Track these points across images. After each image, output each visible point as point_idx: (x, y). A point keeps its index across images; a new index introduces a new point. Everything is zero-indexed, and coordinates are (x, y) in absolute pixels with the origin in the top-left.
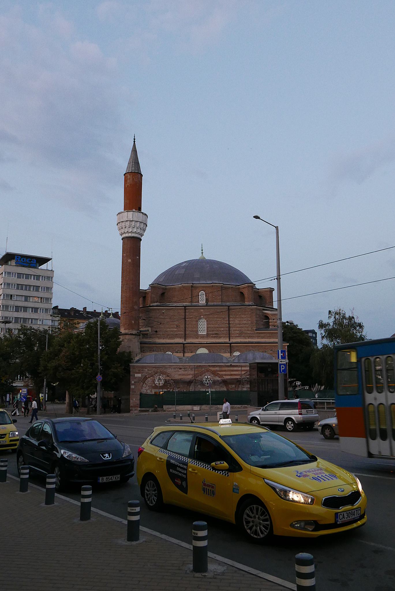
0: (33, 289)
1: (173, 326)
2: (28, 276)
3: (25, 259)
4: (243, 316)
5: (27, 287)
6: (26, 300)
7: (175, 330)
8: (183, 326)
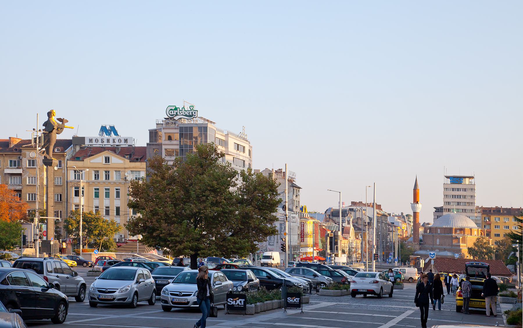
2: (458, 190)
5: (459, 197)
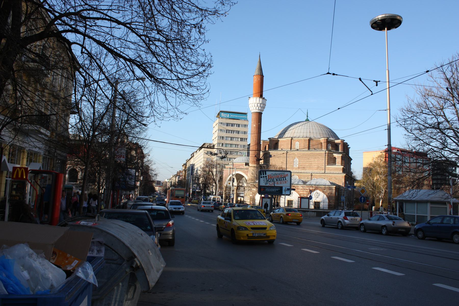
2: (232, 125)
5: (233, 131)
6: (231, 140)
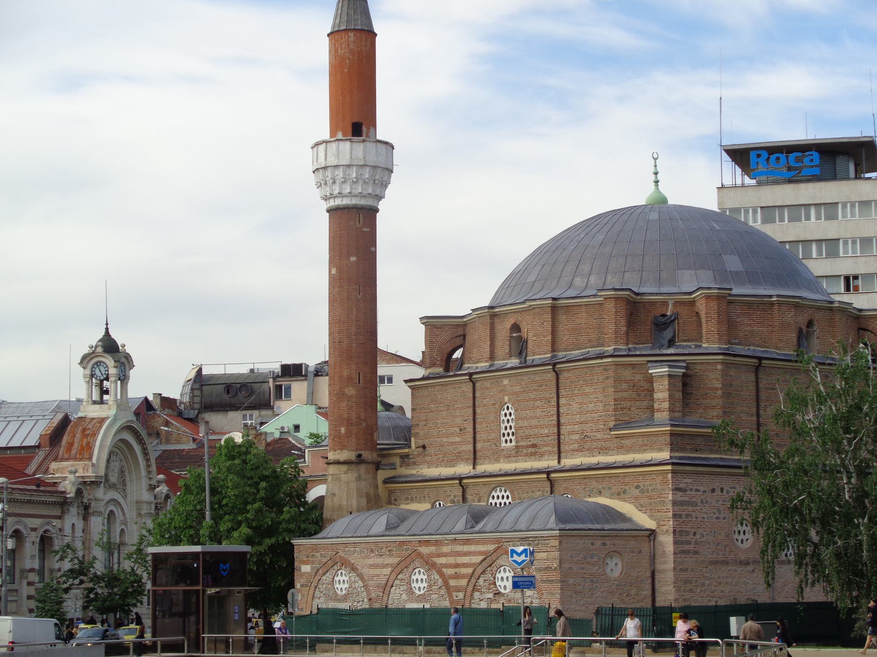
0: (820, 253)
1: (452, 430)
3: (782, 156)
4: (587, 390)
7: (457, 439)
8: (470, 429)
